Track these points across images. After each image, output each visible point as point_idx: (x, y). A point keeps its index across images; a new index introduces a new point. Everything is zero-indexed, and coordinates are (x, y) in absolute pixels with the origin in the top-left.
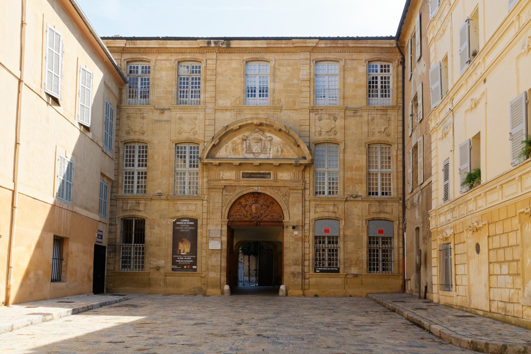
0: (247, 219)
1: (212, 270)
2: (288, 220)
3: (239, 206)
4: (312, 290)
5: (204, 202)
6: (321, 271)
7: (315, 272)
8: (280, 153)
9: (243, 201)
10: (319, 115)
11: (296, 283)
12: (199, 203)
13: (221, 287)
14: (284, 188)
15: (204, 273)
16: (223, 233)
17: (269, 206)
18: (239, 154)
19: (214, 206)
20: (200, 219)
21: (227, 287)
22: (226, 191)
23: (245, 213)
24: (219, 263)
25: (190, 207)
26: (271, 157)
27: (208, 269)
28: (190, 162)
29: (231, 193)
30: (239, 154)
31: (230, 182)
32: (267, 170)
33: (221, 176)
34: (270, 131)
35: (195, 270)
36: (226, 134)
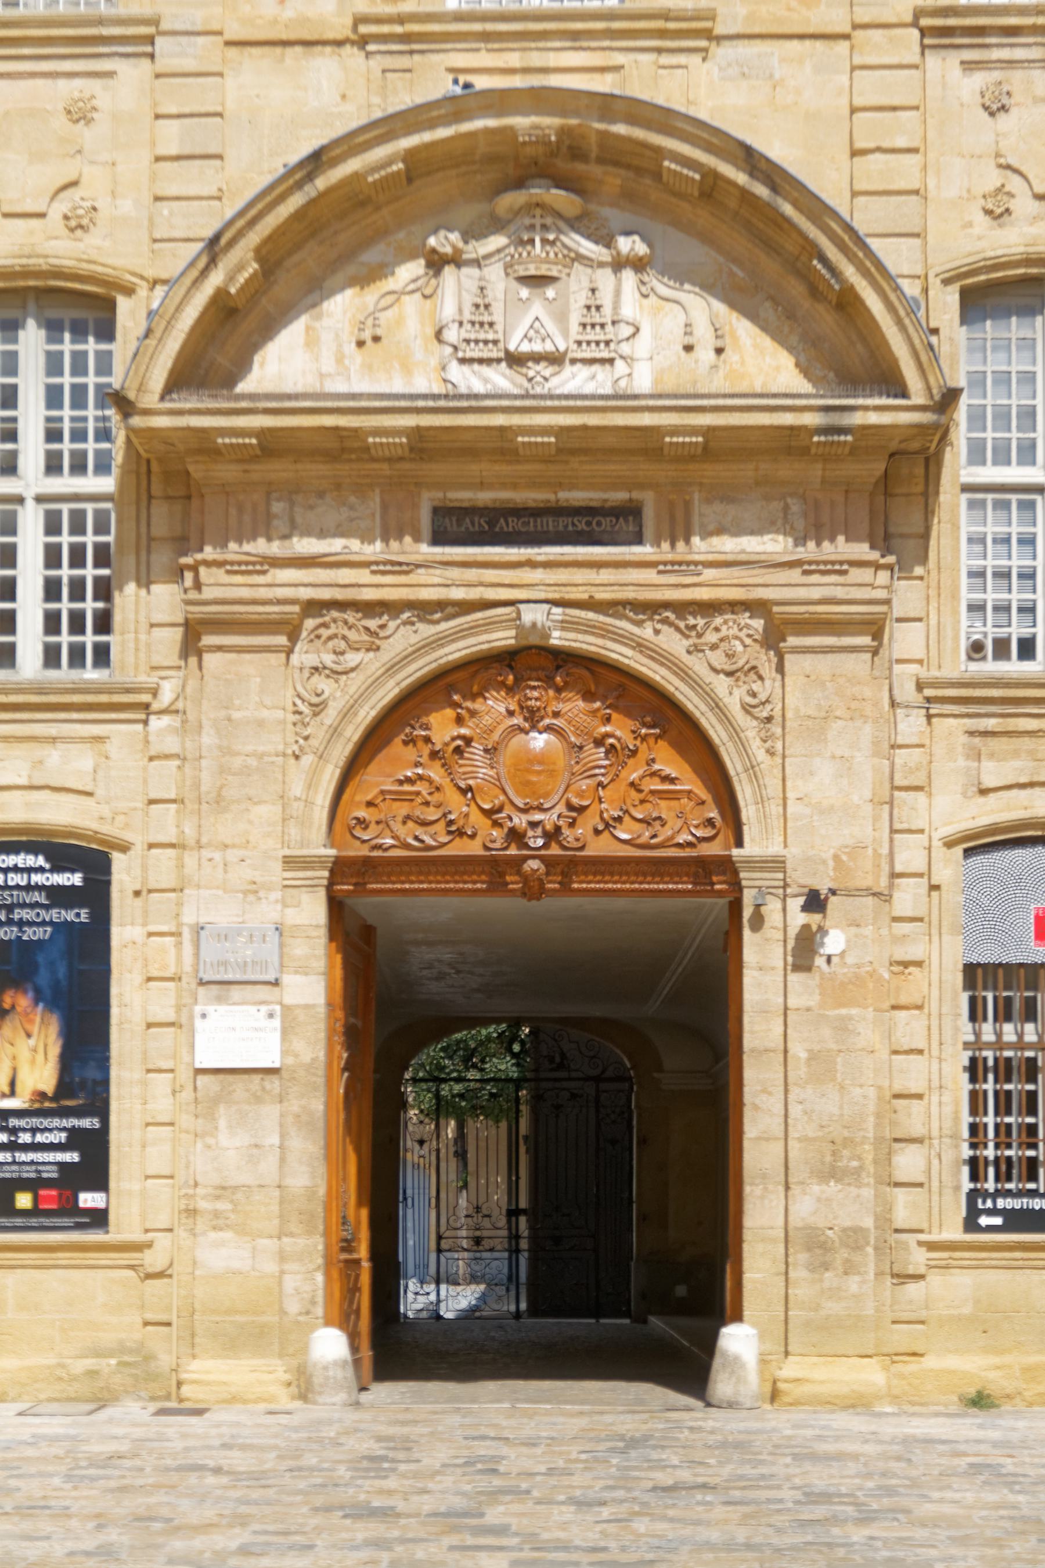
0: (473, 848)
1: (218, 1222)
2: (774, 848)
4: (953, 1362)
5: (156, 723)
6: (1016, 1221)
7: (971, 1224)
8: (705, 355)
10: (997, 75)
11: (832, 1307)
12: (121, 734)
13: (290, 1342)
14: (744, 618)
15: (162, 1241)
16: (299, 949)
18: (407, 370)
19: (227, 751)
20: (124, 848)
21: (331, 1345)
23: (457, 805)
24: (269, 1166)
25: (54, 756)
26: (643, 381)
27: (192, 1212)
28: (53, 435)
29: (352, 658)
30: (407, 370)
31: (345, 575)
32: (614, 487)
34: (629, 198)
35: (99, 1218)
36: (308, 225)
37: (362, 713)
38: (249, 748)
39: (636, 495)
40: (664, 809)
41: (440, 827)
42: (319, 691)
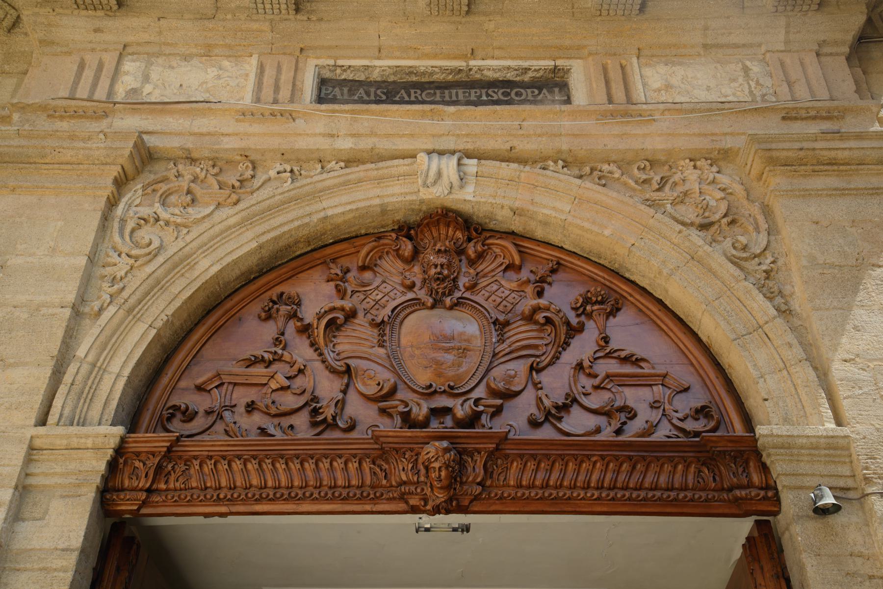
3: (270, 330)
9: (316, 296)
17: (574, 331)
22: (149, 189)
23: (328, 388)
33: (127, 82)
37: (204, 264)
38: (22, 298)
39: (560, 63)
40: (632, 397)
41: (301, 421)
42: (147, 241)
